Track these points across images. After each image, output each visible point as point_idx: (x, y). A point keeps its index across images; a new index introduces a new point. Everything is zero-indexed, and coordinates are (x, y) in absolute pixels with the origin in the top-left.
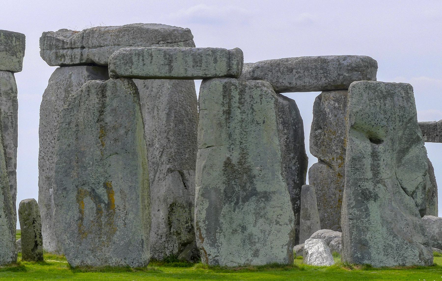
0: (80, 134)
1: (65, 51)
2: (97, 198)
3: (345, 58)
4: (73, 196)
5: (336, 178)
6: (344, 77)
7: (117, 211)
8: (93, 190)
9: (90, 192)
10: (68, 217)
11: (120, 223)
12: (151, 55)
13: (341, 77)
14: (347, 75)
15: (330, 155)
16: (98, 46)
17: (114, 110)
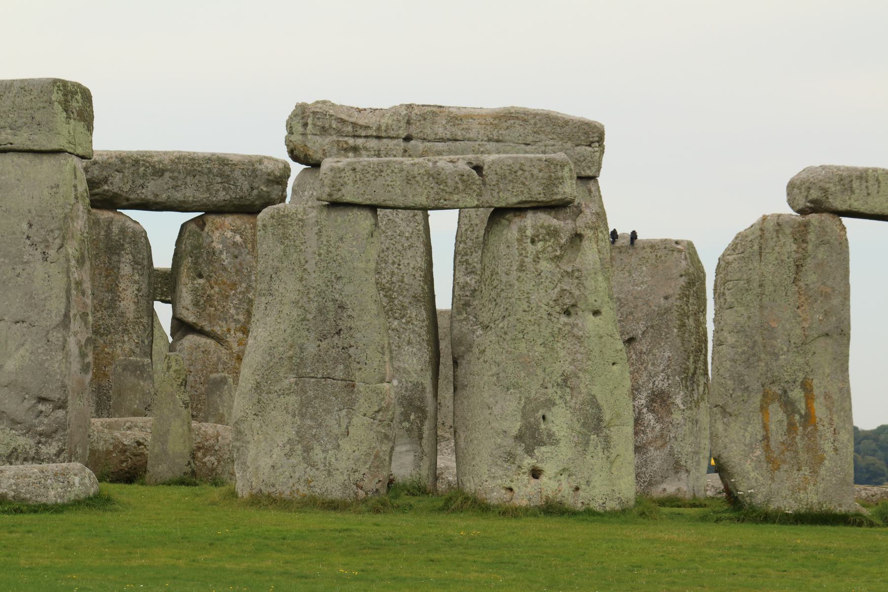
0: (766, 300)
1: (360, 142)
2: (788, 405)
3: (261, 160)
4: (757, 399)
5: (233, 363)
6: (259, 192)
7: (821, 428)
8: (785, 392)
9: (781, 396)
10: (747, 434)
11: (828, 447)
12: (877, 180)
13: (255, 192)
14: (265, 189)
15: (224, 324)
16: (449, 140)
17: (820, 265)
